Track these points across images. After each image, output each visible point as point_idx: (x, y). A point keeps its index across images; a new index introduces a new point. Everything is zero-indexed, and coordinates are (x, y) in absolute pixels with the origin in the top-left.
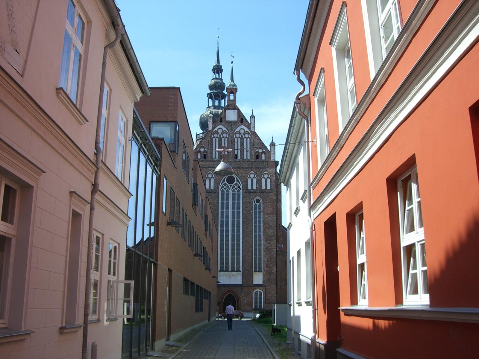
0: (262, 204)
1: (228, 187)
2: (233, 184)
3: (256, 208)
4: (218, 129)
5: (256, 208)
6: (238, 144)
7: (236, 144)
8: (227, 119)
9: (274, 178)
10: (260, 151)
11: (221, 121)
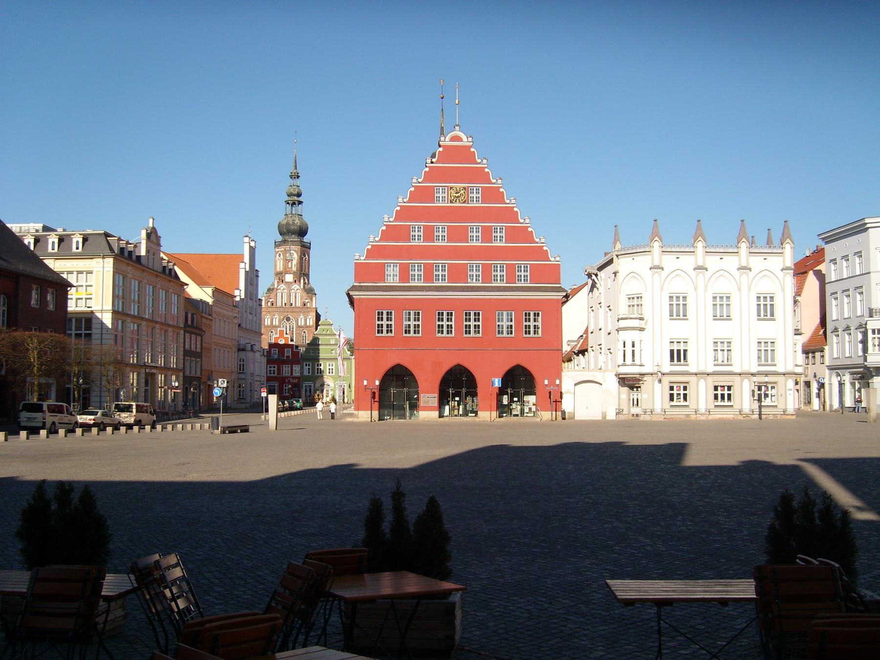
7: (292, 297)
10: (307, 301)
11: (282, 282)
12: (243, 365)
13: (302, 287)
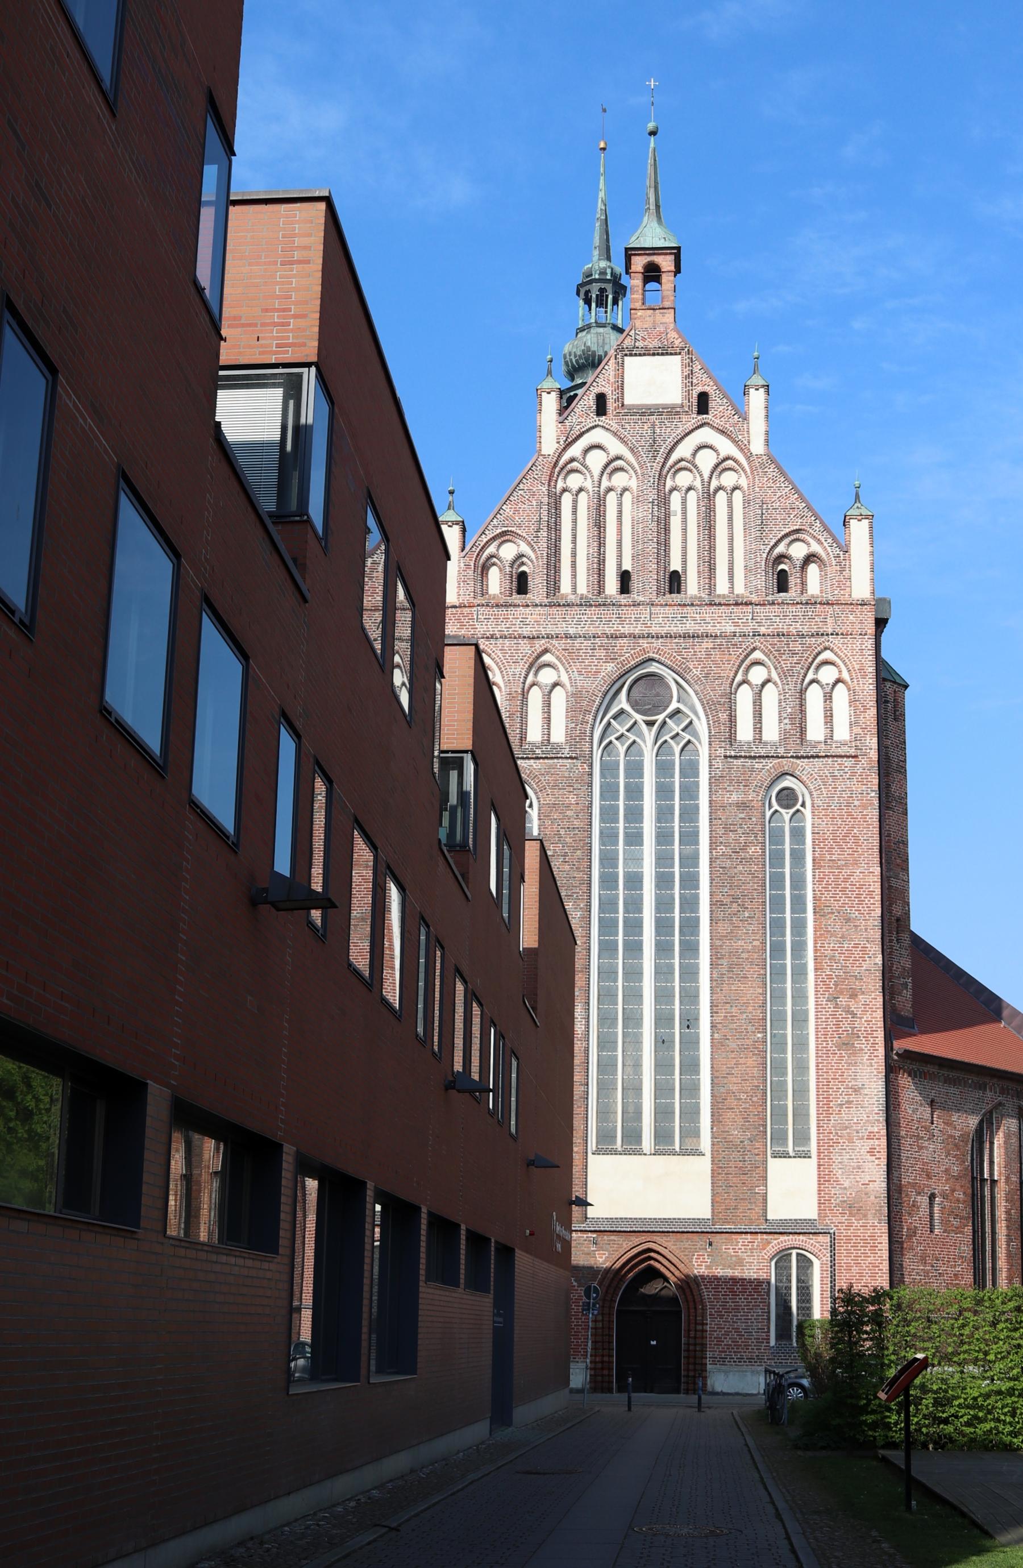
0: (807, 812)
2: (660, 718)
4: (587, 451)
6: (685, 520)
8: (631, 398)
9: (868, 687)
13: (758, 447)
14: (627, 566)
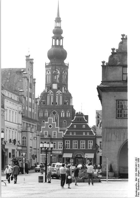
1: (53, 116)
3: (64, 124)
5: (64, 124)
9: (71, 113)
10: (66, 101)
11: (51, 89)
12: (25, 141)
14: (53, 102)
